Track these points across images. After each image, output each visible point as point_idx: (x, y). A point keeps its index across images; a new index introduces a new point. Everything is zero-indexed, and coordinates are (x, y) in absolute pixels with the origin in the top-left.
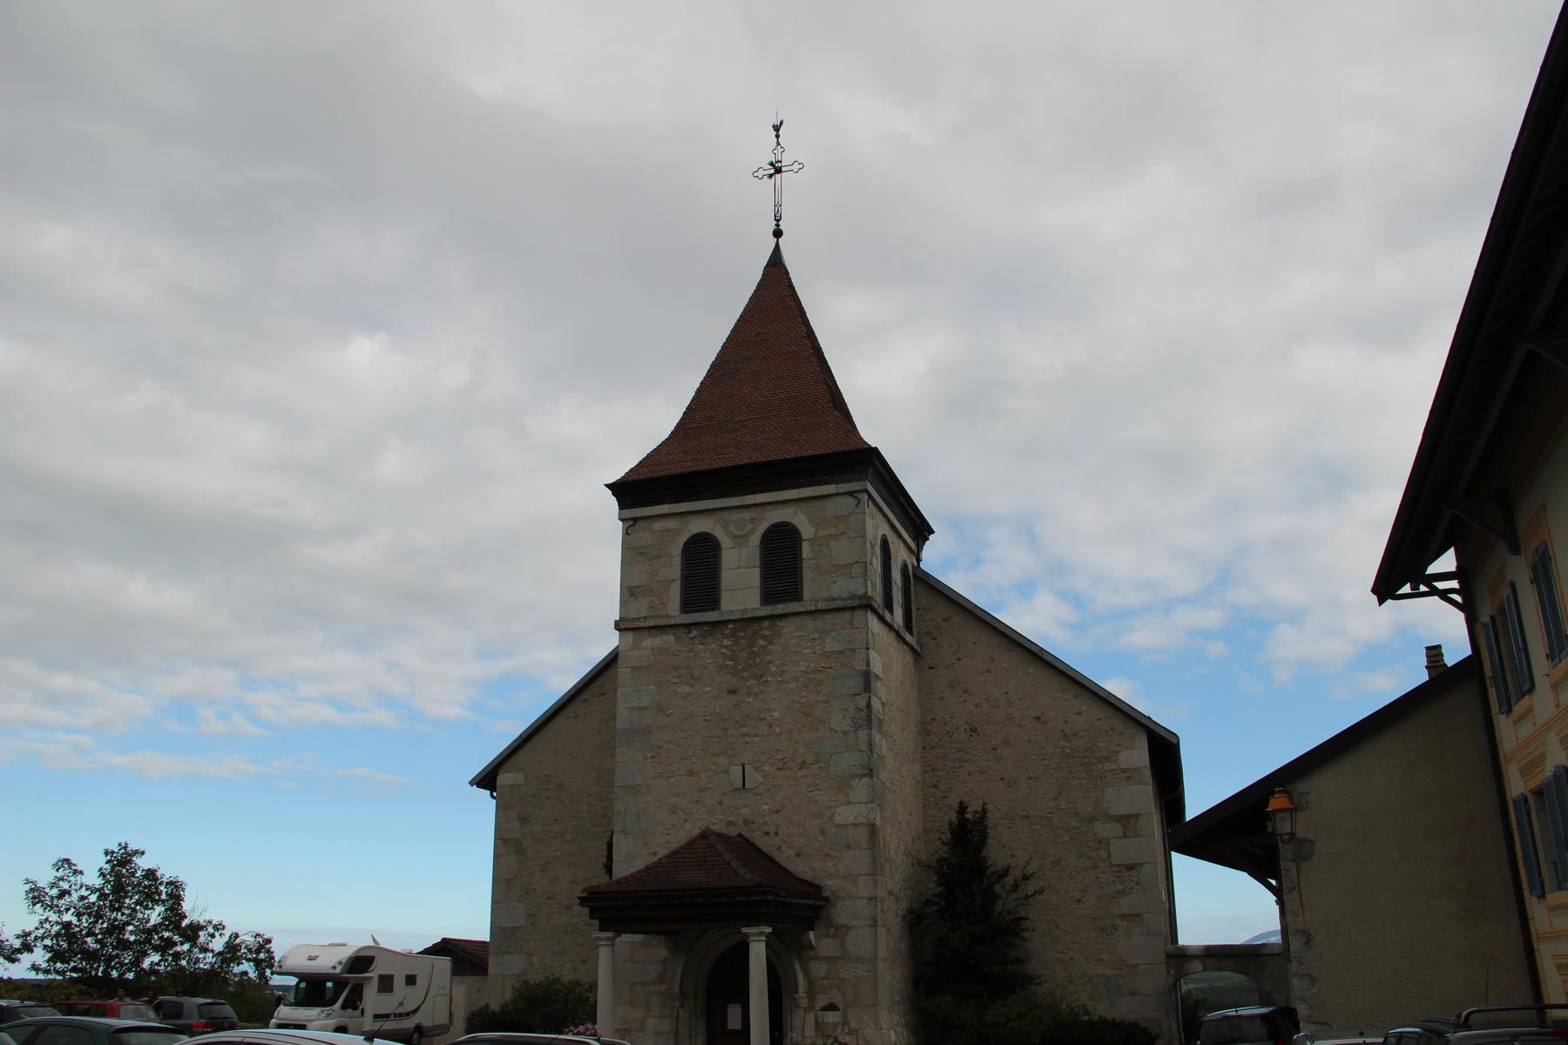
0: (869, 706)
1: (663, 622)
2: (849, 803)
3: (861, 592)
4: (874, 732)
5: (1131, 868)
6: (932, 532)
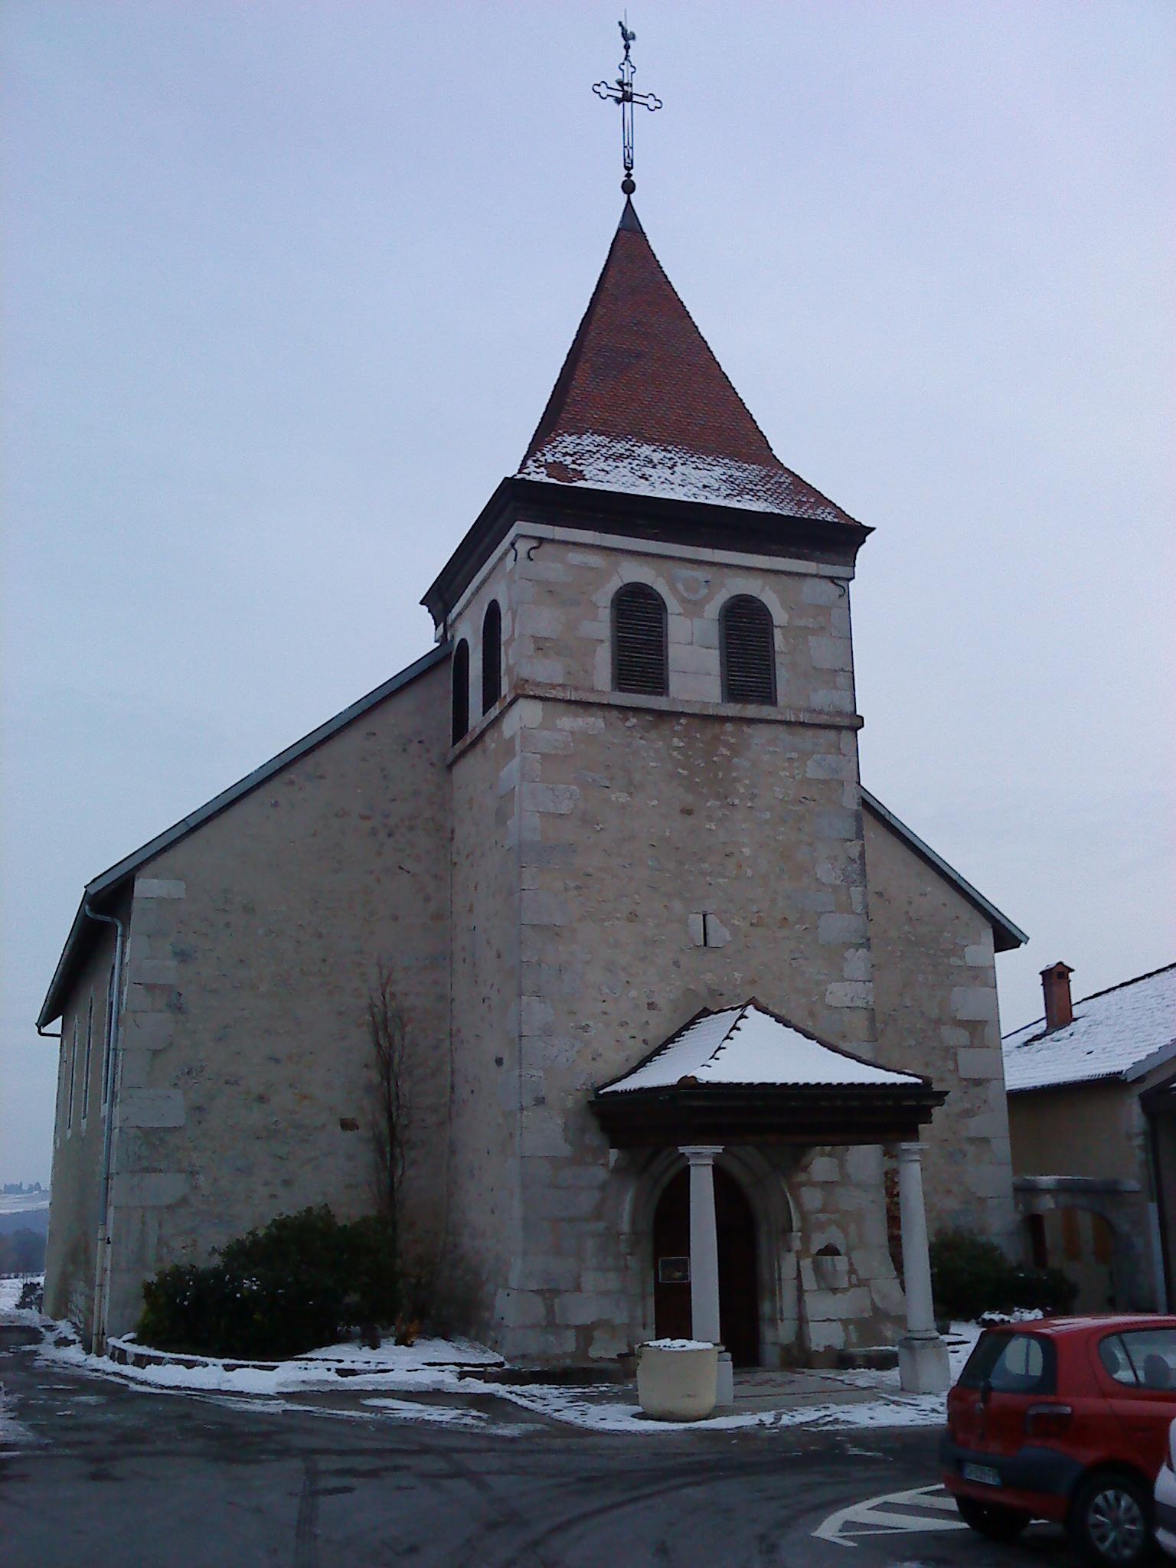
2: (843, 980)
3: (849, 709)
5: (978, 1082)
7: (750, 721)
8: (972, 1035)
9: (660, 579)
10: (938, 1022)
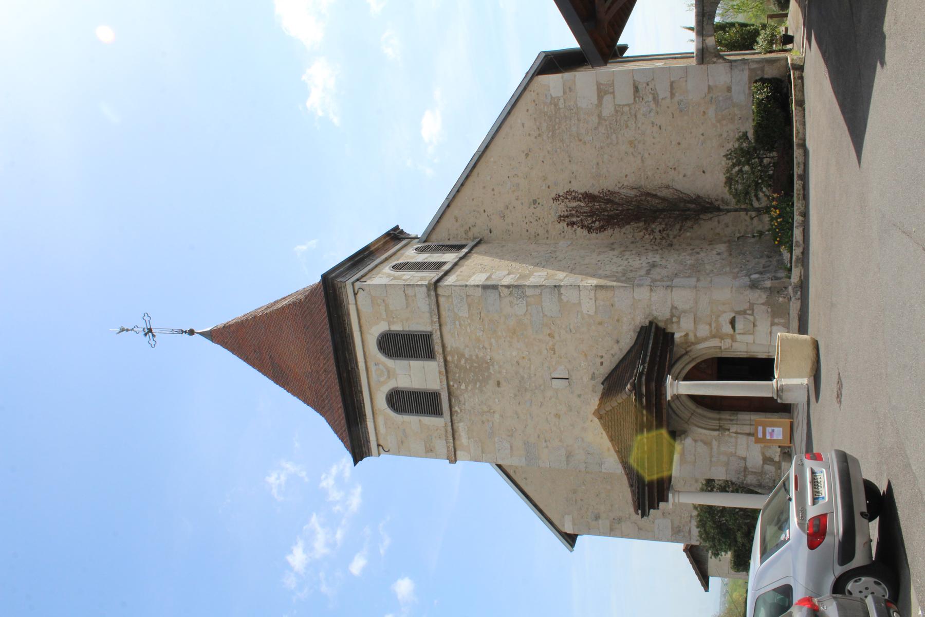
0: (508, 287)
1: (450, 429)
2: (580, 304)
3: (425, 289)
4: (527, 283)
5: (636, 89)
6: (397, 228)
7: (443, 346)
8: (606, 93)
9: (381, 389)
10: (600, 116)
